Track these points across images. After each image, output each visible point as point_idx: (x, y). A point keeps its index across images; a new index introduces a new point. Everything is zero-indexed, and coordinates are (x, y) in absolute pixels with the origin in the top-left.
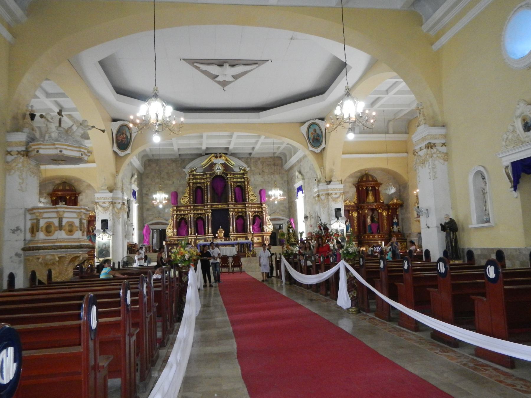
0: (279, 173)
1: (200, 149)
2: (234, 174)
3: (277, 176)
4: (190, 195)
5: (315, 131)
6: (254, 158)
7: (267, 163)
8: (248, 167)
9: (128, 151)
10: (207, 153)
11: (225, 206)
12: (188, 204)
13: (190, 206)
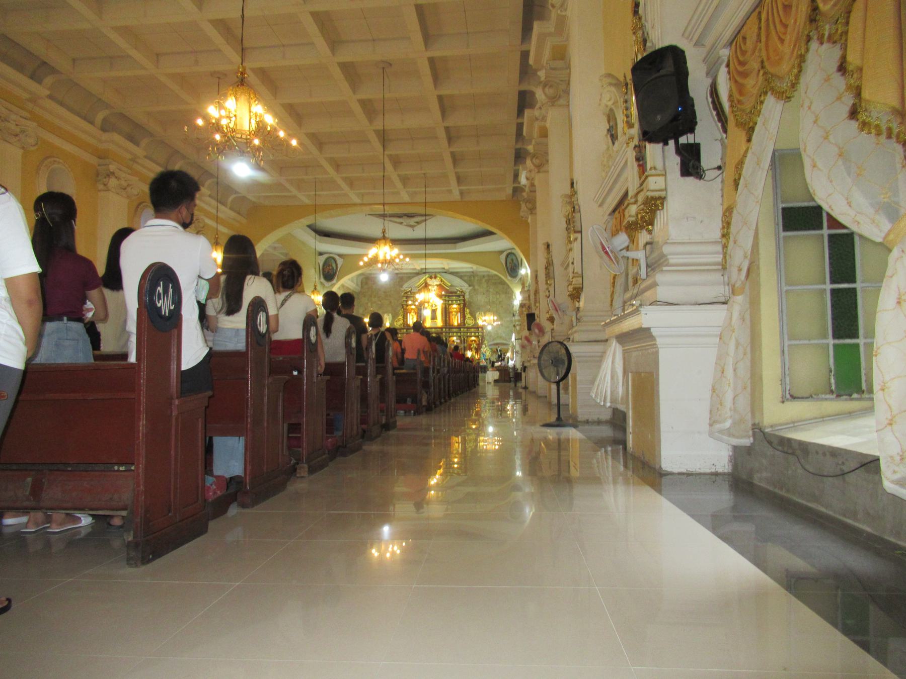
0: (506, 293)
1: (415, 269)
2: (449, 296)
3: (503, 296)
4: (403, 317)
5: (512, 260)
6: (477, 275)
7: (493, 281)
8: (470, 286)
9: (335, 281)
10: (423, 272)
11: (439, 330)
12: (402, 326)
13: (403, 329)
